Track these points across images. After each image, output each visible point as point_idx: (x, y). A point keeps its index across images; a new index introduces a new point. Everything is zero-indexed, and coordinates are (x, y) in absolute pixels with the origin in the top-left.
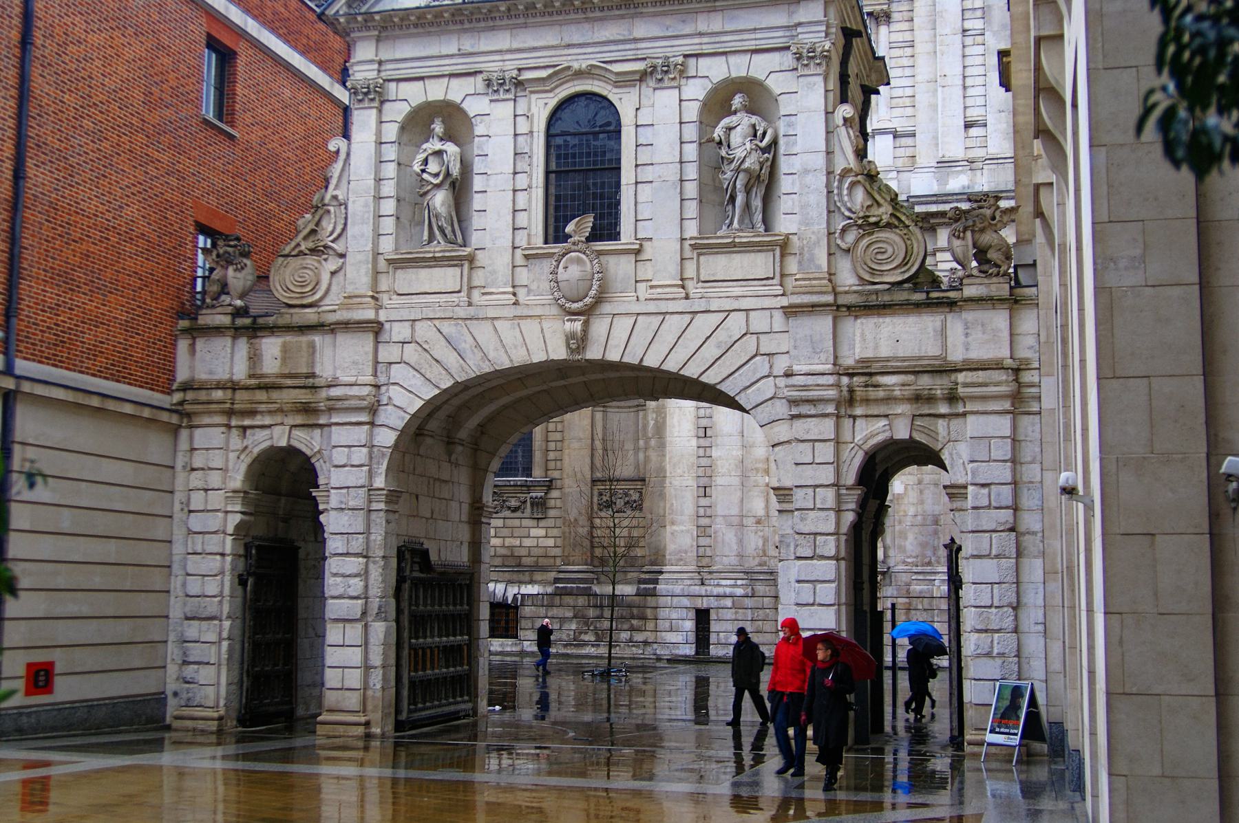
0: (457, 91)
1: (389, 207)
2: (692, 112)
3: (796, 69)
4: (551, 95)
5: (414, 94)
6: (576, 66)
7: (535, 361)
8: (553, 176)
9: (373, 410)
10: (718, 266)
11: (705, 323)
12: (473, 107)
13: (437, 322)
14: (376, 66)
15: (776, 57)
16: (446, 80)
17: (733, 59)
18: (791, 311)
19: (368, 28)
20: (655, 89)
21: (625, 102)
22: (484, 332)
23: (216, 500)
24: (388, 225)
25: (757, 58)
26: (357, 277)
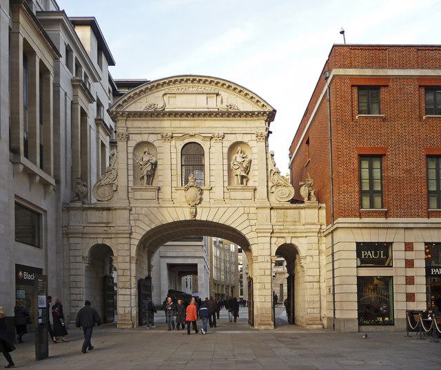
2: (226, 150)
5: (139, 139)
6: (191, 134)
7: (181, 220)
8: (184, 168)
9: (131, 234)
10: (234, 194)
11: (231, 211)
12: (156, 144)
16: (147, 135)
21: (205, 145)
26: (122, 193)
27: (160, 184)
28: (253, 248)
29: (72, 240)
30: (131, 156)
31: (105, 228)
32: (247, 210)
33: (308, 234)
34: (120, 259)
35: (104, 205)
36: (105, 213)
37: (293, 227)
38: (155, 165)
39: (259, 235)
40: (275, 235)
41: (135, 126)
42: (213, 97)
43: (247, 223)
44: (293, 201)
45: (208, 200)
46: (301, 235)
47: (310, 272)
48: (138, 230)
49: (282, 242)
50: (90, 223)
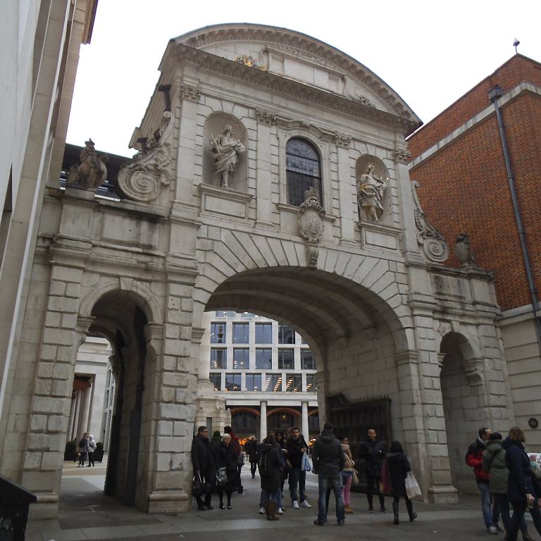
0: (239, 112)
1: (200, 161)
2: (353, 163)
3: (394, 160)
4: (288, 132)
5: (216, 106)
12: (248, 123)
13: (233, 232)
14: (198, 82)
15: (385, 151)
17: (368, 145)
18: (408, 265)
19: (194, 61)
20: (337, 147)
21: (325, 148)
22: (261, 242)
23: (70, 321)
24: (200, 171)
25: (378, 150)
26: (184, 193)
27: (251, 192)
28: (409, 332)
29: (58, 273)
30: (200, 131)
31: (143, 258)
32: (393, 266)
33: (481, 321)
34: (171, 331)
35: (142, 208)
36: (145, 226)
37: (458, 306)
38: (241, 157)
39: (416, 312)
40: (437, 316)
41: (210, 83)
42: (336, 81)
43: (393, 289)
44: (445, 263)
45: (331, 238)
46: (471, 321)
47: (495, 388)
48: (209, 272)
49: (447, 328)
50: (108, 240)
